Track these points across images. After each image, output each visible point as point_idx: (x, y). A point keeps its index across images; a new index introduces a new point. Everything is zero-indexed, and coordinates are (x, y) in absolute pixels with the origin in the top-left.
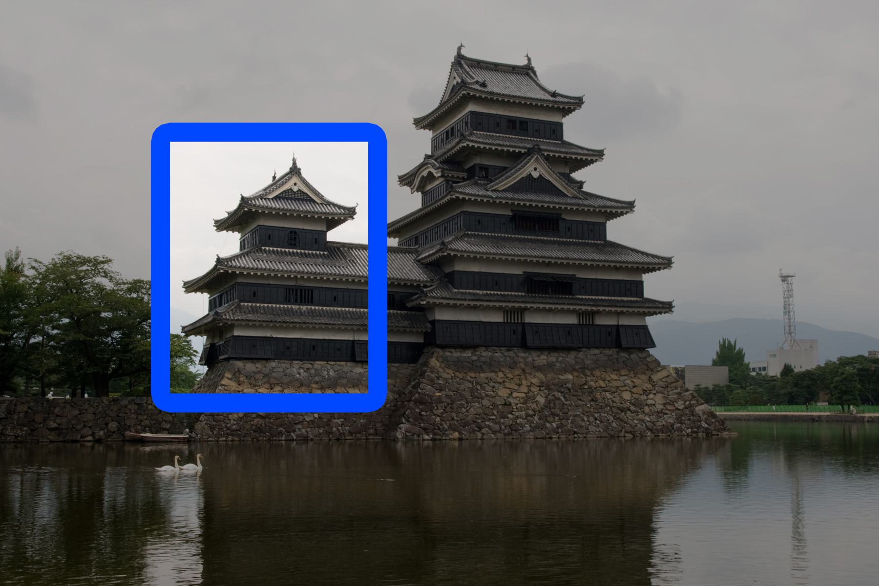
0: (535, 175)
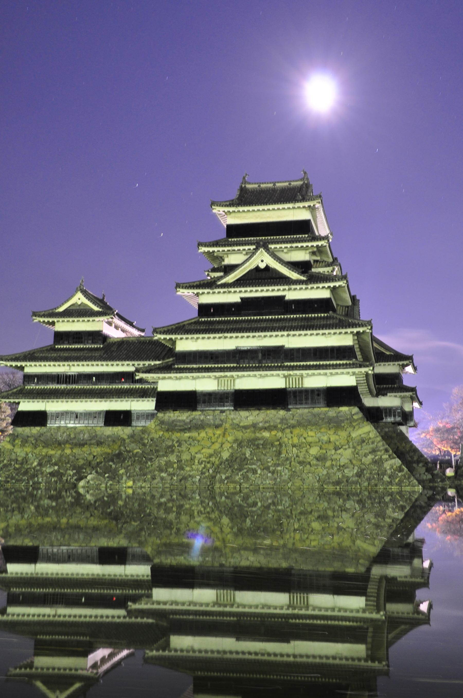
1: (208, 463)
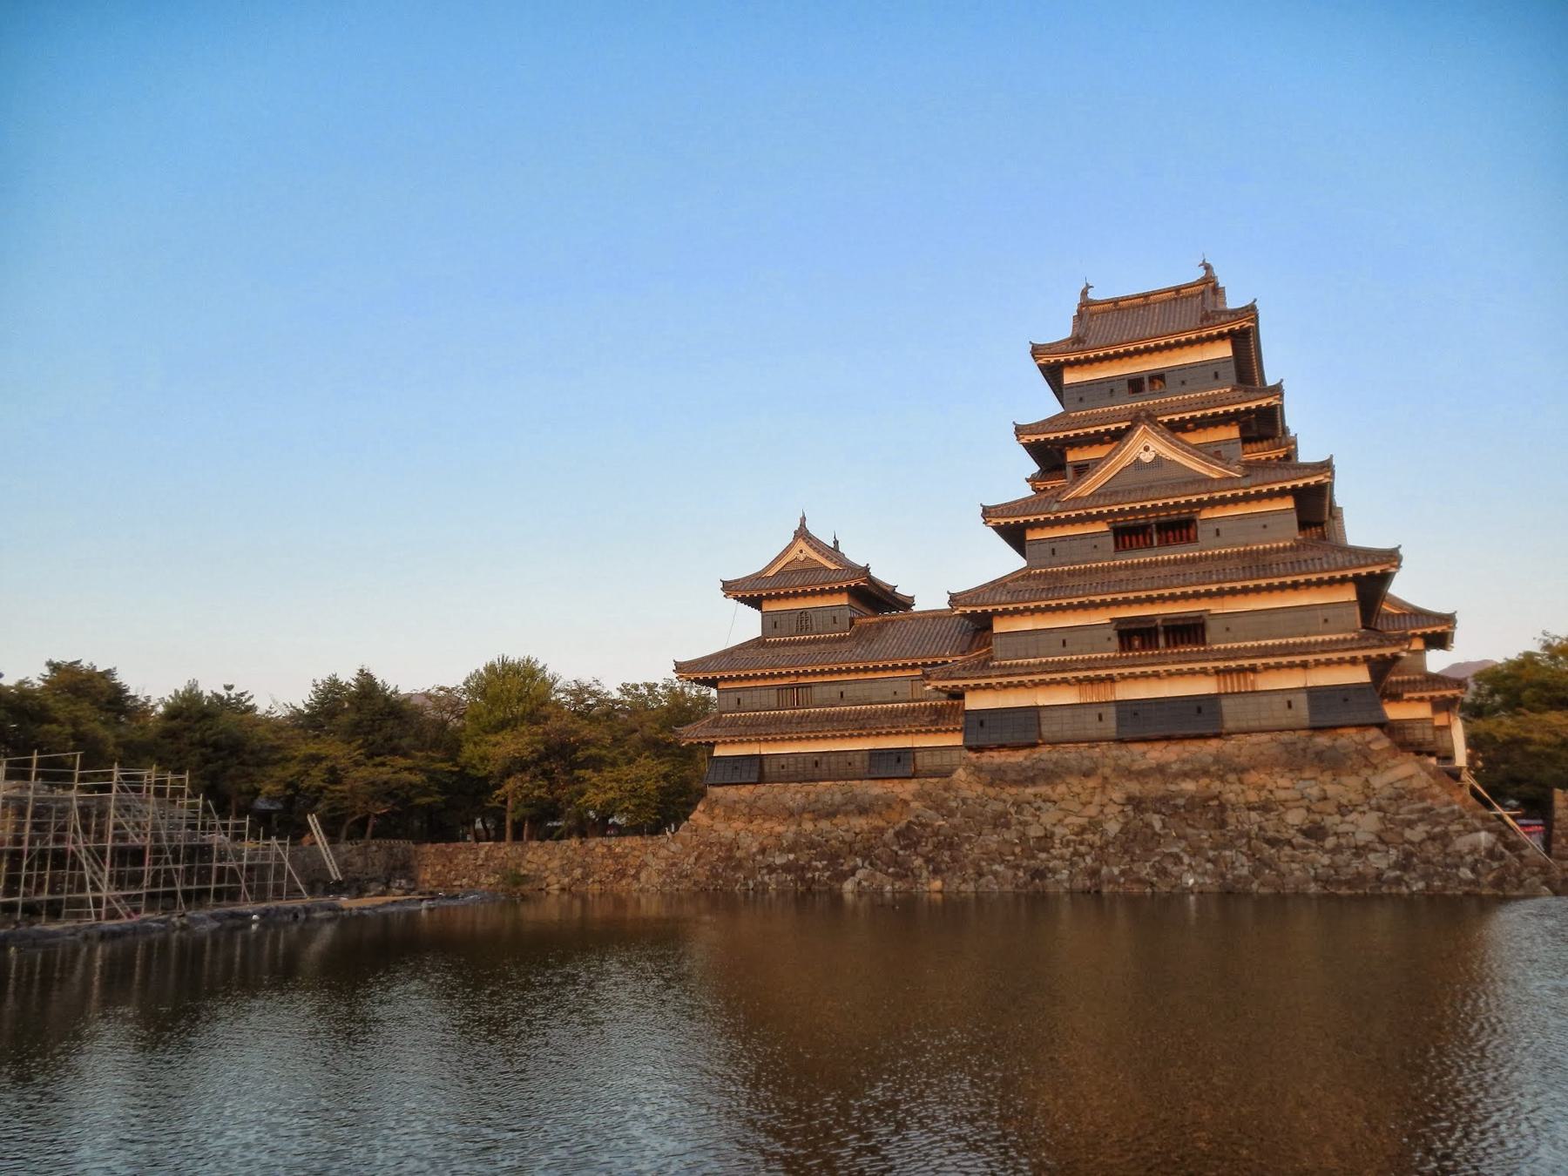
0: (1147, 457)
1: (1081, 843)
